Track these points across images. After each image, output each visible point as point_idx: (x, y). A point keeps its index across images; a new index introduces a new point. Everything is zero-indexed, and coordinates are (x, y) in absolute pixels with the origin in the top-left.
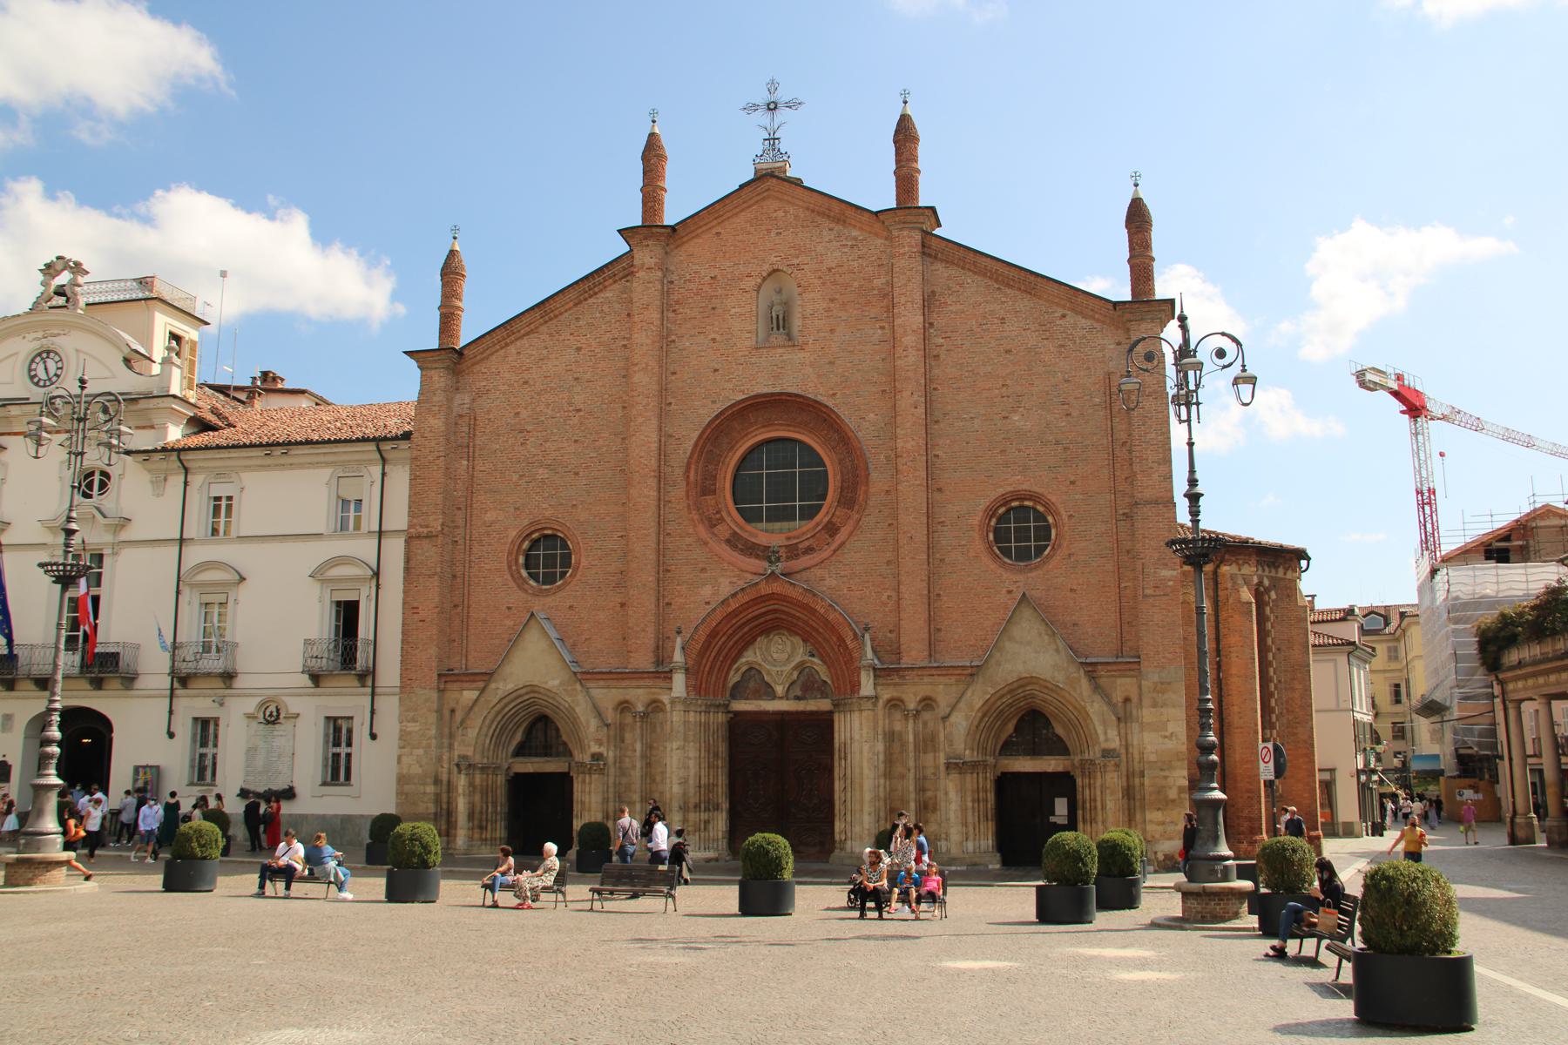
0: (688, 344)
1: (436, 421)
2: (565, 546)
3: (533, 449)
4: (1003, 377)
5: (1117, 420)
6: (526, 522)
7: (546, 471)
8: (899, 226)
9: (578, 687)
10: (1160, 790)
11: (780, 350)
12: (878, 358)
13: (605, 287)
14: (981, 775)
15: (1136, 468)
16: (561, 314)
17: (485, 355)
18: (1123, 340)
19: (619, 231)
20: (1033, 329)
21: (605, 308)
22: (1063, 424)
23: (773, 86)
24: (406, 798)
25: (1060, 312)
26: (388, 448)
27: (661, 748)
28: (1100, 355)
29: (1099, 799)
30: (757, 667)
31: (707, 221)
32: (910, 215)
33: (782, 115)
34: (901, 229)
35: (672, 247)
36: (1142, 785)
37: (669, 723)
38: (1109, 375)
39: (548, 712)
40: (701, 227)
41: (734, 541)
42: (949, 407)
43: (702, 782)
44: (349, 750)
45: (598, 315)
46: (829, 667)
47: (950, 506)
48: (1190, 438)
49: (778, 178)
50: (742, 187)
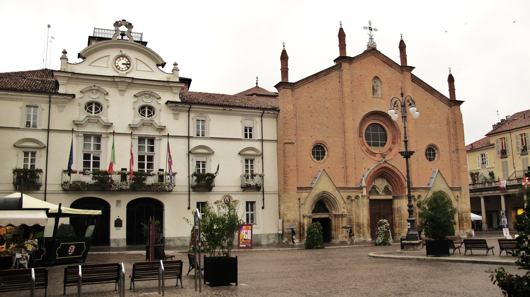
1: (290, 106)
2: (322, 148)
3: (314, 118)
6: (314, 141)
7: (319, 126)
9: (337, 191)
11: (379, 99)
23: (370, 23)
25: (437, 100)
33: (373, 32)
34: (407, 72)
41: (368, 150)
44: (248, 213)
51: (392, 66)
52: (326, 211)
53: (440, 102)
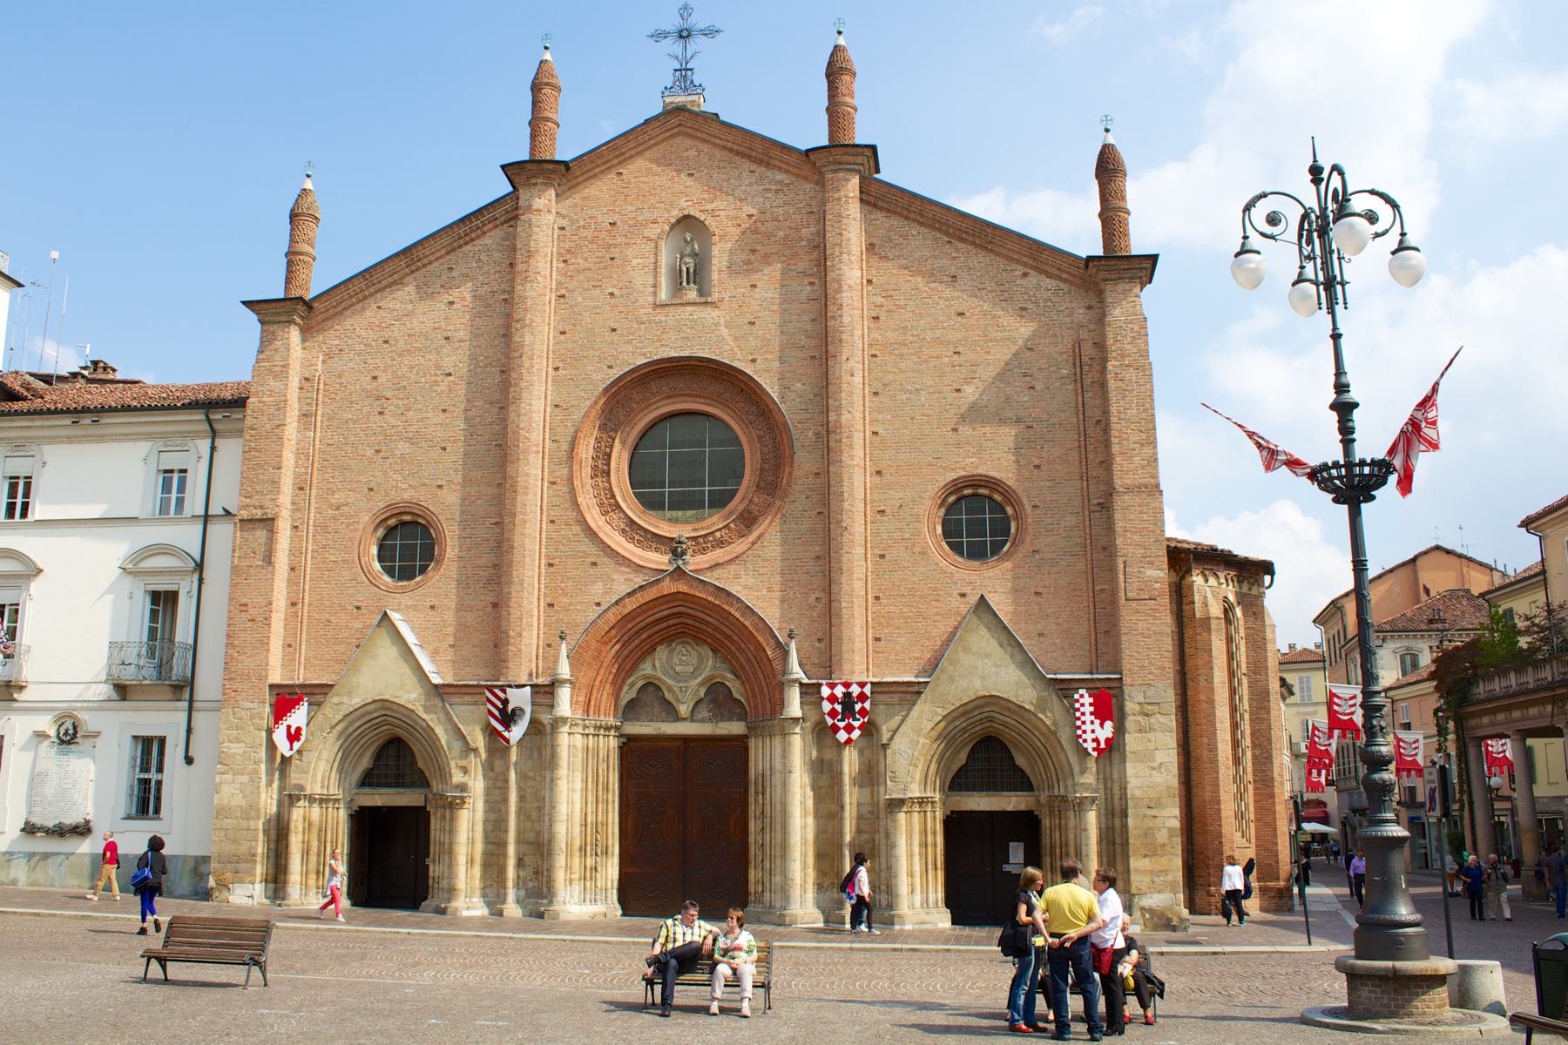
0: (580, 299)
3: (392, 420)
4: (954, 343)
5: (1090, 394)
6: (381, 505)
7: (407, 445)
8: (832, 167)
10: (1147, 833)
11: (689, 308)
12: (806, 319)
13: (484, 233)
14: (929, 814)
15: (1115, 449)
16: (430, 263)
17: (339, 309)
18: (1094, 304)
19: (503, 167)
20: (990, 289)
21: (484, 257)
22: (1025, 399)
23: (685, 10)
24: (226, 835)
25: (1020, 270)
26: (219, 416)
27: (538, 778)
28: (1068, 320)
29: (1072, 844)
30: (656, 682)
31: (607, 158)
32: (846, 154)
34: (836, 171)
35: (564, 188)
36: (1125, 826)
37: (549, 748)
38: (1078, 344)
39: (401, 733)
40: (599, 166)
42: (891, 377)
43: (589, 820)
45: (475, 265)
46: (743, 683)
47: (891, 492)
48: (1335, 328)
49: (691, 112)
50: (647, 122)
51: (772, 162)
52: (422, 782)
53: (1034, 278)
